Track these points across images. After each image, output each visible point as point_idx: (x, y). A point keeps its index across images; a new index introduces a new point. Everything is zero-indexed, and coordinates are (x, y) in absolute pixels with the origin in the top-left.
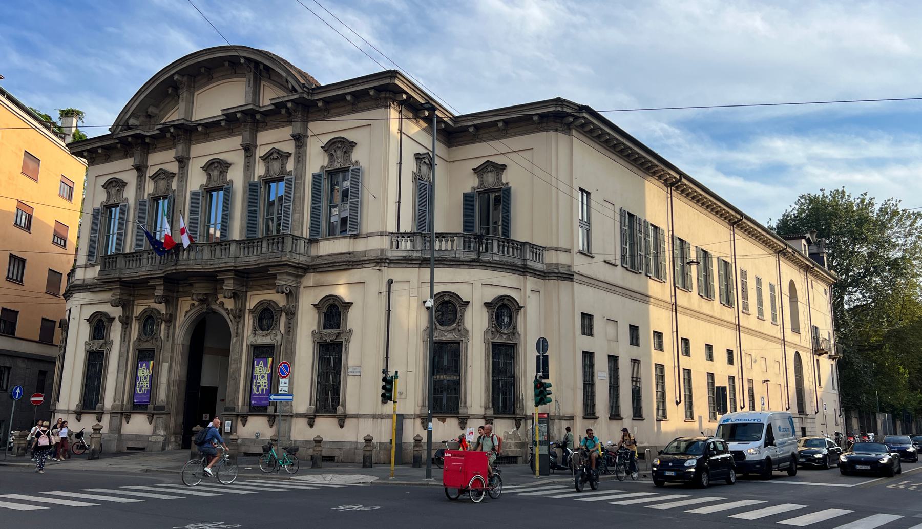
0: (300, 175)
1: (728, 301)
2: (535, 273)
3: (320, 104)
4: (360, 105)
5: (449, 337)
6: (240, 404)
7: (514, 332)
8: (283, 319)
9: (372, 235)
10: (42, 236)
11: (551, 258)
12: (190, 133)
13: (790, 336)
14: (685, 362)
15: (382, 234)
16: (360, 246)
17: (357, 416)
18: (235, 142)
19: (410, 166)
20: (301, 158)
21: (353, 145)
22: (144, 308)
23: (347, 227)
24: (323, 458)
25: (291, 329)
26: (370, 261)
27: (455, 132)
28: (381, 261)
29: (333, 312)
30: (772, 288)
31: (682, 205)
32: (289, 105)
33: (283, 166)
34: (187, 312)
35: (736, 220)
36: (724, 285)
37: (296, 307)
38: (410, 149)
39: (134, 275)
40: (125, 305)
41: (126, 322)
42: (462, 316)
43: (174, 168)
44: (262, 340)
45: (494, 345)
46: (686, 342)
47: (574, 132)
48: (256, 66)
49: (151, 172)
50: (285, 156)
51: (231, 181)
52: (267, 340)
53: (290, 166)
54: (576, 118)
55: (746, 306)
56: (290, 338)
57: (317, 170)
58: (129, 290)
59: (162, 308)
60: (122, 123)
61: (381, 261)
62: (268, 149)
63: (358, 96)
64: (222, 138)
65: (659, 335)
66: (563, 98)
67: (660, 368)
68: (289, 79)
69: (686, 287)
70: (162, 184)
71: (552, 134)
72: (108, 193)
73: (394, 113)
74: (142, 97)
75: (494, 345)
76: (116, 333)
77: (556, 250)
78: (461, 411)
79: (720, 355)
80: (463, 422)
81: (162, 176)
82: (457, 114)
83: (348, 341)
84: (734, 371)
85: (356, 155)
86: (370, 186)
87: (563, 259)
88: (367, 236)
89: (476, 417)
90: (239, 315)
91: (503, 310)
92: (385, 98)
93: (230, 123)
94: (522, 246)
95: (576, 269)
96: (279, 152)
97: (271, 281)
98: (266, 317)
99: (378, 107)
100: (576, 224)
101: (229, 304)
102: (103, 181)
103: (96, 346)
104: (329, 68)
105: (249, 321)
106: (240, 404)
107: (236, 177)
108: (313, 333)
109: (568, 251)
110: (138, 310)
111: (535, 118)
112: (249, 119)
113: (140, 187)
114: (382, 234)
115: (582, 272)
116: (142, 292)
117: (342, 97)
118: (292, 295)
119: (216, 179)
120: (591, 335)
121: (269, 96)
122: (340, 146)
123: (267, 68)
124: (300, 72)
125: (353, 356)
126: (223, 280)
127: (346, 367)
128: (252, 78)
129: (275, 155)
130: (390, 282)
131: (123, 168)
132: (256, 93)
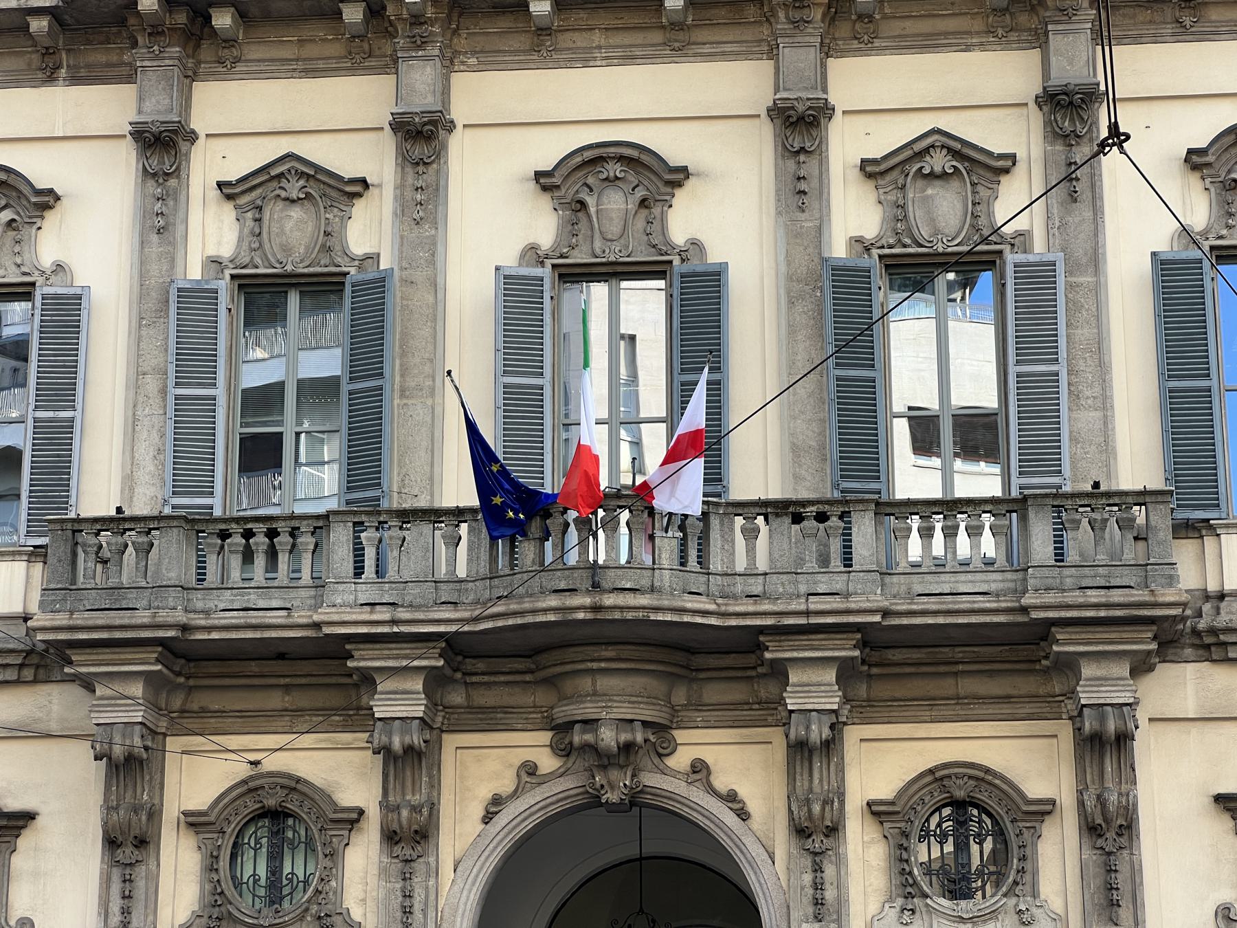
8: (1058, 858)
20: (1073, 184)
22: (241, 770)
33: (977, 208)
34: (497, 801)
50: (981, 168)
51: (696, 244)
53: (1016, 205)
64: (629, 59)
81: (294, 188)
90: (816, 831)
97: (766, 690)
105: (864, 857)
110: (199, 776)
116: (214, 701)
118: (1105, 746)
119: (614, 229)
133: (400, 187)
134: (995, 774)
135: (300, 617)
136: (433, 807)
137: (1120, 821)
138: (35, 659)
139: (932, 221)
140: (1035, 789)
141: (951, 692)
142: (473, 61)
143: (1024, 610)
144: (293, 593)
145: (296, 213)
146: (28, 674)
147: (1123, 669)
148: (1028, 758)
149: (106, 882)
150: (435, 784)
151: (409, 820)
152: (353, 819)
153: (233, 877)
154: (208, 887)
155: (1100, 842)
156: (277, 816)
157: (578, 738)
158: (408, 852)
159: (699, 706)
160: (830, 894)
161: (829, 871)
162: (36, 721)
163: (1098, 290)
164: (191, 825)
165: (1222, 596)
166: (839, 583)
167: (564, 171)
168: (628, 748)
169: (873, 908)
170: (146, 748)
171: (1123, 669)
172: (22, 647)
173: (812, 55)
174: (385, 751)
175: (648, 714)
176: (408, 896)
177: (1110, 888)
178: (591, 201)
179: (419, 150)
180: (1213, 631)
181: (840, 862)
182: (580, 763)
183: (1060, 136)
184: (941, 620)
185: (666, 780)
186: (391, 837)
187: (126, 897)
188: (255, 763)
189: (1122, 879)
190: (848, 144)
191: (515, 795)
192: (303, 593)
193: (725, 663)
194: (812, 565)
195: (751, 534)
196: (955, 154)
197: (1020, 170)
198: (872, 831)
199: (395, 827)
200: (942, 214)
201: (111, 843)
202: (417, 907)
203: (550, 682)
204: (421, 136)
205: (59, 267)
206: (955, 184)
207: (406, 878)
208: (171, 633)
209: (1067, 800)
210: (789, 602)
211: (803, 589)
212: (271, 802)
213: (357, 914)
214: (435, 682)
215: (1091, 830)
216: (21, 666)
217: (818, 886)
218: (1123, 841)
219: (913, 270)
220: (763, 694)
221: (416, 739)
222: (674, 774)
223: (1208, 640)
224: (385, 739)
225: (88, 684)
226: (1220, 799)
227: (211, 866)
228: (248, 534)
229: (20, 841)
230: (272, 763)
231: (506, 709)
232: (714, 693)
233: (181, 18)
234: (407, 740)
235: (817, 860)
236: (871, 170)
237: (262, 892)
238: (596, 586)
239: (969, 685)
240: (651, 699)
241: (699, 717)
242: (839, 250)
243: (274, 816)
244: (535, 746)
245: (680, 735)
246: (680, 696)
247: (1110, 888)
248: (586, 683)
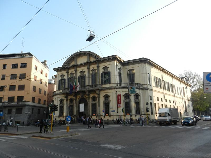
0: (99, 73)
1: (172, 91)
2: (141, 89)
3: (102, 61)
4: (109, 61)
5: (128, 101)
6: (90, 114)
7: (139, 100)
8: (97, 99)
9: (113, 84)
10: (43, 84)
11: (144, 86)
12: (76, 66)
13: (184, 97)
14: (166, 103)
15: (115, 83)
16: (111, 85)
17: (113, 115)
18: (86, 67)
19: (118, 71)
20: (98, 70)
21: (108, 68)
23: (109, 81)
24: (108, 123)
26: (113, 88)
27: (124, 64)
28: (115, 88)
29: (107, 97)
30: (180, 88)
31: (164, 75)
32: (96, 61)
33: (95, 72)
35: (173, 76)
36: (171, 88)
37: (100, 97)
38: (118, 68)
40: (67, 97)
41: (67, 100)
42: (130, 98)
43: (74, 72)
45: (136, 102)
46: (166, 100)
47: (146, 63)
48: (90, 54)
49: (70, 73)
50: (95, 70)
53: (97, 71)
54: (146, 61)
55: (175, 92)
57: (102, 72)
58: (67, 95)
59: (74, 98)
60: (64, 65)
61: (115, 88)
62: (92, 69)
63: (109, 59)
65: (162, 99)
66: (144, 58)
67: (162, 105)
68: (96, 57)
69: (165, 89)
70: (72, 75)
71: (142, 64)
72: (61, 77)
73: (115, 62)
75: (136, 102)
76: (65, 102)
77: (145, 84)
78: (131, 114)
79: (172, 102)
80: (131, 116)
82: (125, 61)
83: (110, 102)
84: (174, 104)
86: (112, 74)
87: (146, 86)
88: (112, 84)
89: (133, 115)
90: (89, 99)
91: (137, 96)
92: (114, 59)
93: (85, 64)
94: (138, 84)
95: (148, 88)
96: (94, 69)
98: (94, 99)
99: (113, 61)
100: (148, 80)
101: (87, 97)
102: (60, 75)
103: (61, 105)
104: (103, 55)
105: (91, 100)
106: (90, 114)
107: (86, 73)
109: (147, 85)
110: (69, 98)
111: (139, 61)
112: (88, 64)
113: (68, 76)
114: (115, 83)
115: (150, 88)
117: (106, 59)
118: (99, 95)
120: (151, 99)
121: (92, 59)
122: (106, 68)
123: (91, 54)
124: (97, 55)
126: (86, 92)
127: (110, 107)
128: (88, 56)
129: (94, 70)
130: (117, 92)
131: (64, 72)
132: (89, 59)
230: (72, 97)
235: (89, 100)
236: (91, 70)
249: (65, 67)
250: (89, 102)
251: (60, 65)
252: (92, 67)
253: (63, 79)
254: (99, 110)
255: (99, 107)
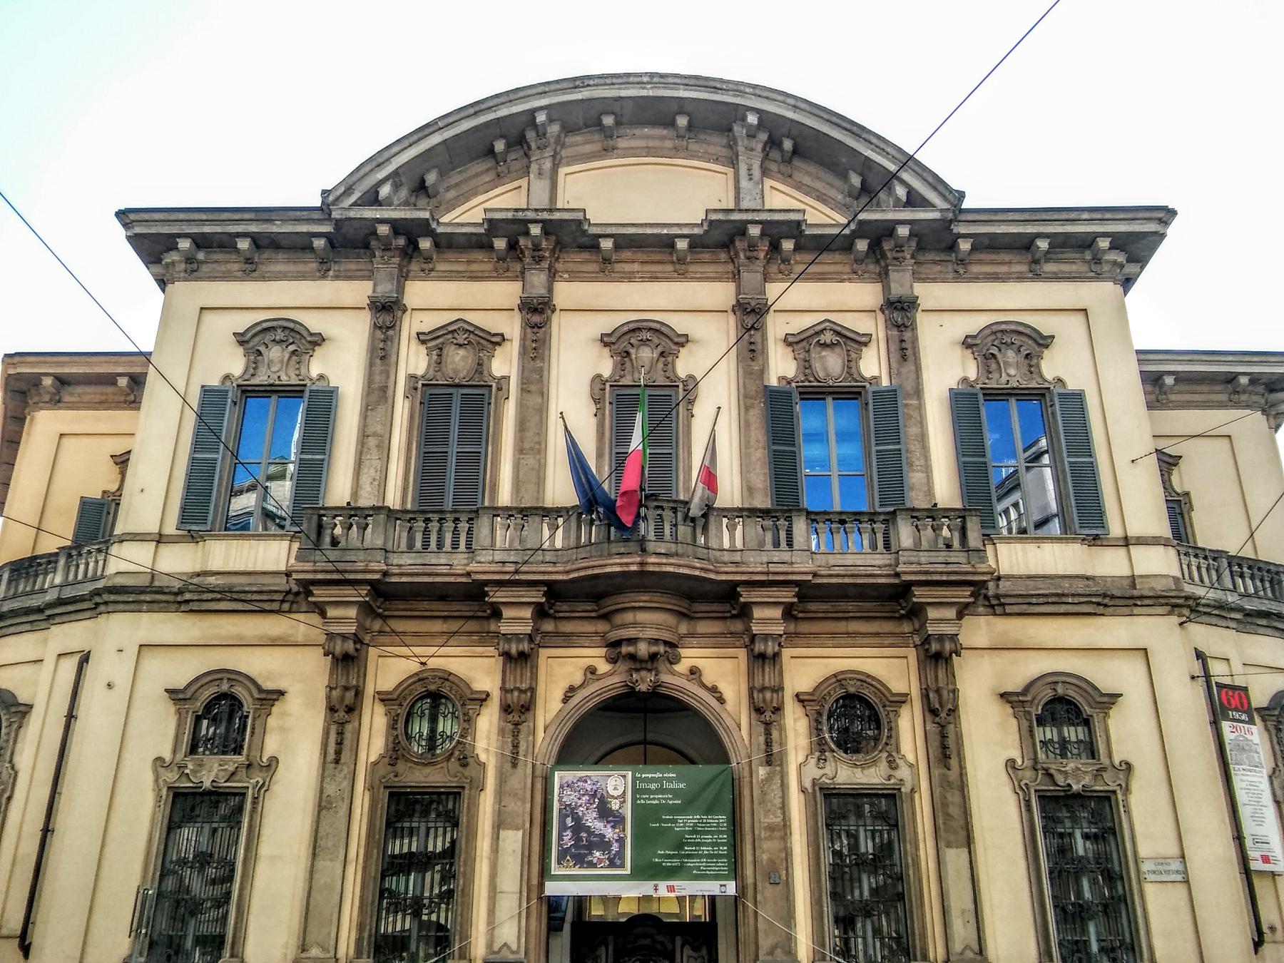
8: (909, 729)
9: (1142, 541)
22: (413, 666)
25: (945, 749)
33: (850, 364)
34: (572, 690)
39: (444, 570)
41: (343, 710)
44: (847, 773)
50: (851, 342)
52: (872, 776)
56: (953, 774)
60: (361, 186)
63: (1062, 244)
74: (436, 139)
83: (1127, 790)
85: (1052, 366)
88: (1126, 542)
90: (765, 710)
105: (796, 728)
108: (1010, 763)
110: (390, 669)
125: (1147, 827)
133: (523, 339)
134: (874, 678)
135: (459, 570)
136: (532, 690)
137: (950, 706)
138: (290, 597)
139: (825, 369)
140: (897, 686)
141: (844, 630)
142: (566, 276)
143: (897, 575)
144: (454, 556)
145: (462, 352)
146: (286, 606)
147: (951, 613)
148: (891, 668)
149: (326, 733)
150: (534, 676)
151: (519, 697)
152: (483, 698)
153: (406, 733)
154: (391, 739)
155: (937, 719)
156: (436, 698)
157: (625, 649)
158: (517, 718)
159: (692, 635)
160: (776, 749)
161: (775, 734)
162: (289, 635)
163: (920, 408)
164: (382, 700)
165: (999, 578)
166: (786, 556)
167: (617, 334)
168: (653, 657)
169: (801, 759)
170: (357, 650)
171: (951, 613)
172: (282, 589)
173: (759, 277)
174: (507, 655)
175: (666, 636)
176: (516, 746)
177: (944, 747)
178: (633, 351)
179: (536, 319)
180: (997, 597)
181: (782, 729)
182: (622, 667)
183: (893, 325)
184: (847, 580)
185: (674, 679)
186: (506, 709)
187: (340, 743)
188: (423, 664)
189: (951, 741)
190: (777, 327)
191: (582, 686)
192: (460, 556)
193: (716, 601)
194: (769, 546)
195: (732, 529)
196: (838, 334)
197: (873, 345)
198: (799, 710)
199: (510, 702)
200: (830, 365)
201: (332, 709)
202: (521, 753)
203: (606, 617)
204: (537, 311)
205: (321, 377)
206: (838, 350)
207: (516, 734)
208: (377, 576)
209: (915, 693)
210: (756, 564)
211: (765, 559)
212: (432, 687)
213: (483, 757)
214: (541, 612)
215: (931, 711)
216: (283, 601)
217: (768, 743)
218: (950, 719)
219: (814, 393)
220: (733, 629)
221: (525, 646)
222: (680, 675)
223: (994, 602)
224: (507, 647)
225: (320, 609)
226: (1003, 696)
227: (392, 726)
228: (427, 520)
229: (274, 709)
230: (433, 663)
231: (578, 635)
232: (703, 627)
233: (401, 241)
234: (521, 648)
237: (424, 743)
238: (644, 550)
239: (854, 626)
240: (669, 629)
241: (694, 641)
242: (773, 382)
243: (434, 697)
244: (596, 657)
245: (684, 652)
246: (683, 628)
247: (944, 747)
248: (629, 617)
249: (369, 213)
250: (772, 757)
251: (296, 171)
252: (800, 301)
253: (296, 392)
254: (960, 899)
255: (956, 858)
